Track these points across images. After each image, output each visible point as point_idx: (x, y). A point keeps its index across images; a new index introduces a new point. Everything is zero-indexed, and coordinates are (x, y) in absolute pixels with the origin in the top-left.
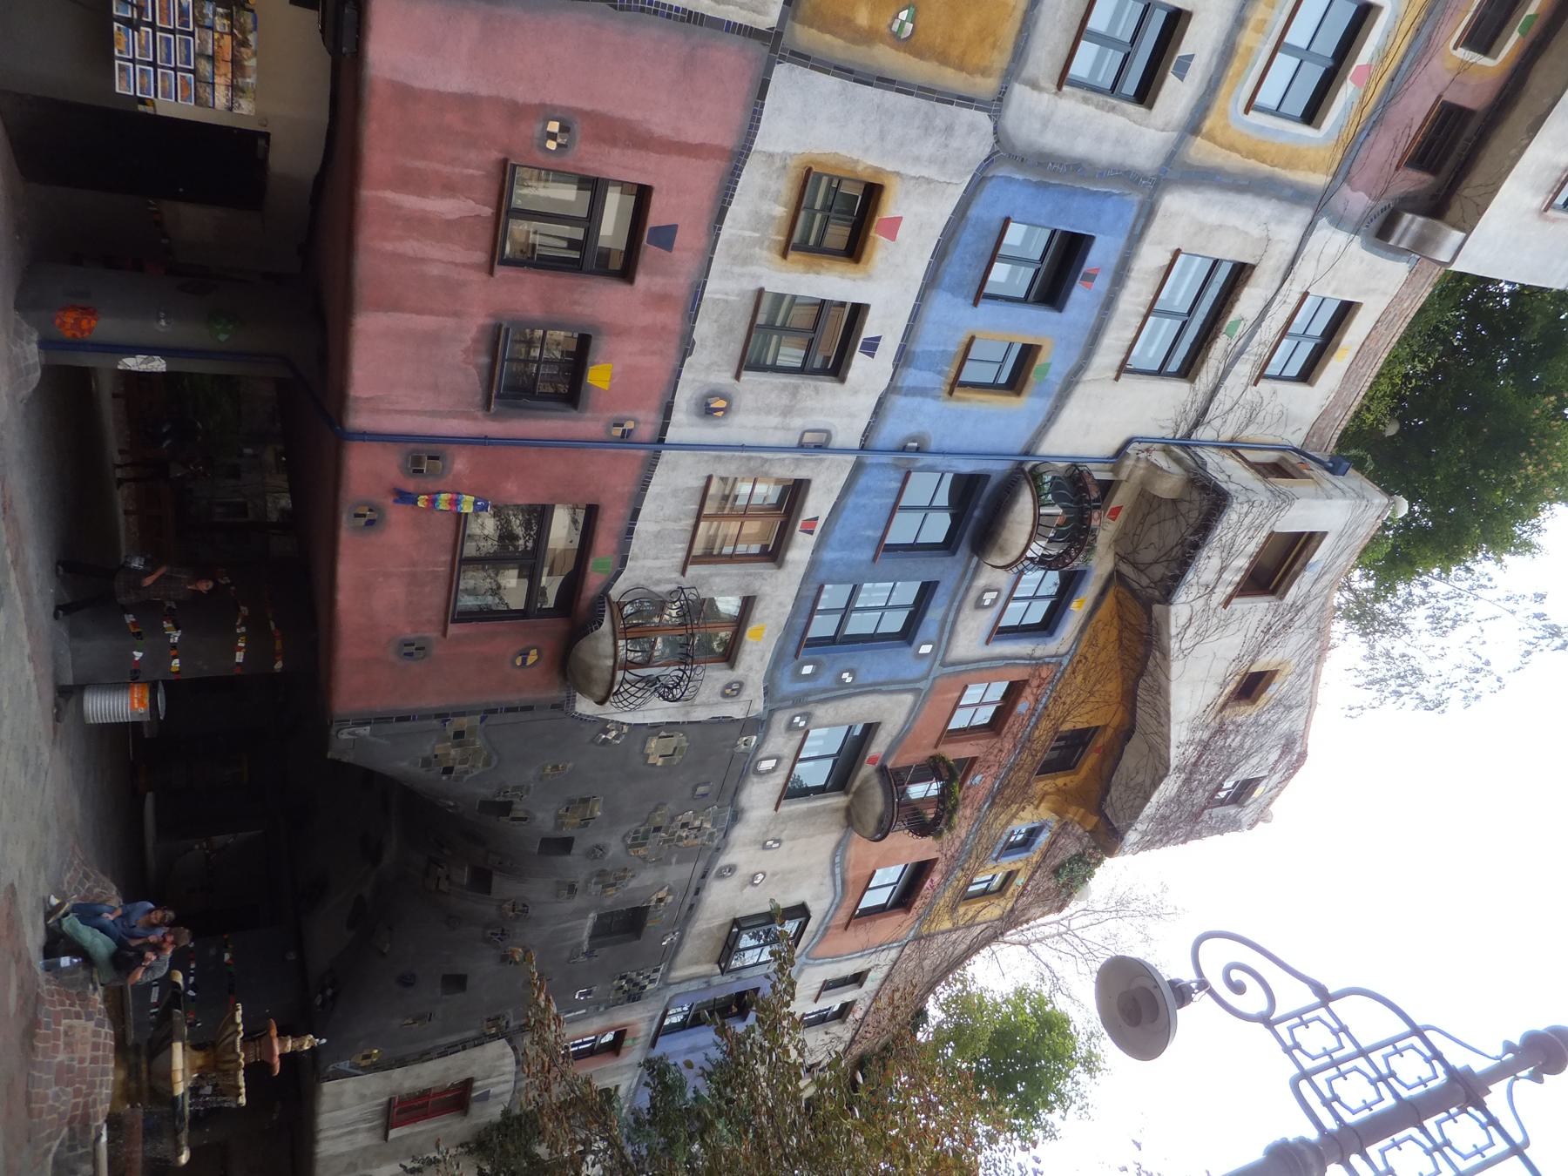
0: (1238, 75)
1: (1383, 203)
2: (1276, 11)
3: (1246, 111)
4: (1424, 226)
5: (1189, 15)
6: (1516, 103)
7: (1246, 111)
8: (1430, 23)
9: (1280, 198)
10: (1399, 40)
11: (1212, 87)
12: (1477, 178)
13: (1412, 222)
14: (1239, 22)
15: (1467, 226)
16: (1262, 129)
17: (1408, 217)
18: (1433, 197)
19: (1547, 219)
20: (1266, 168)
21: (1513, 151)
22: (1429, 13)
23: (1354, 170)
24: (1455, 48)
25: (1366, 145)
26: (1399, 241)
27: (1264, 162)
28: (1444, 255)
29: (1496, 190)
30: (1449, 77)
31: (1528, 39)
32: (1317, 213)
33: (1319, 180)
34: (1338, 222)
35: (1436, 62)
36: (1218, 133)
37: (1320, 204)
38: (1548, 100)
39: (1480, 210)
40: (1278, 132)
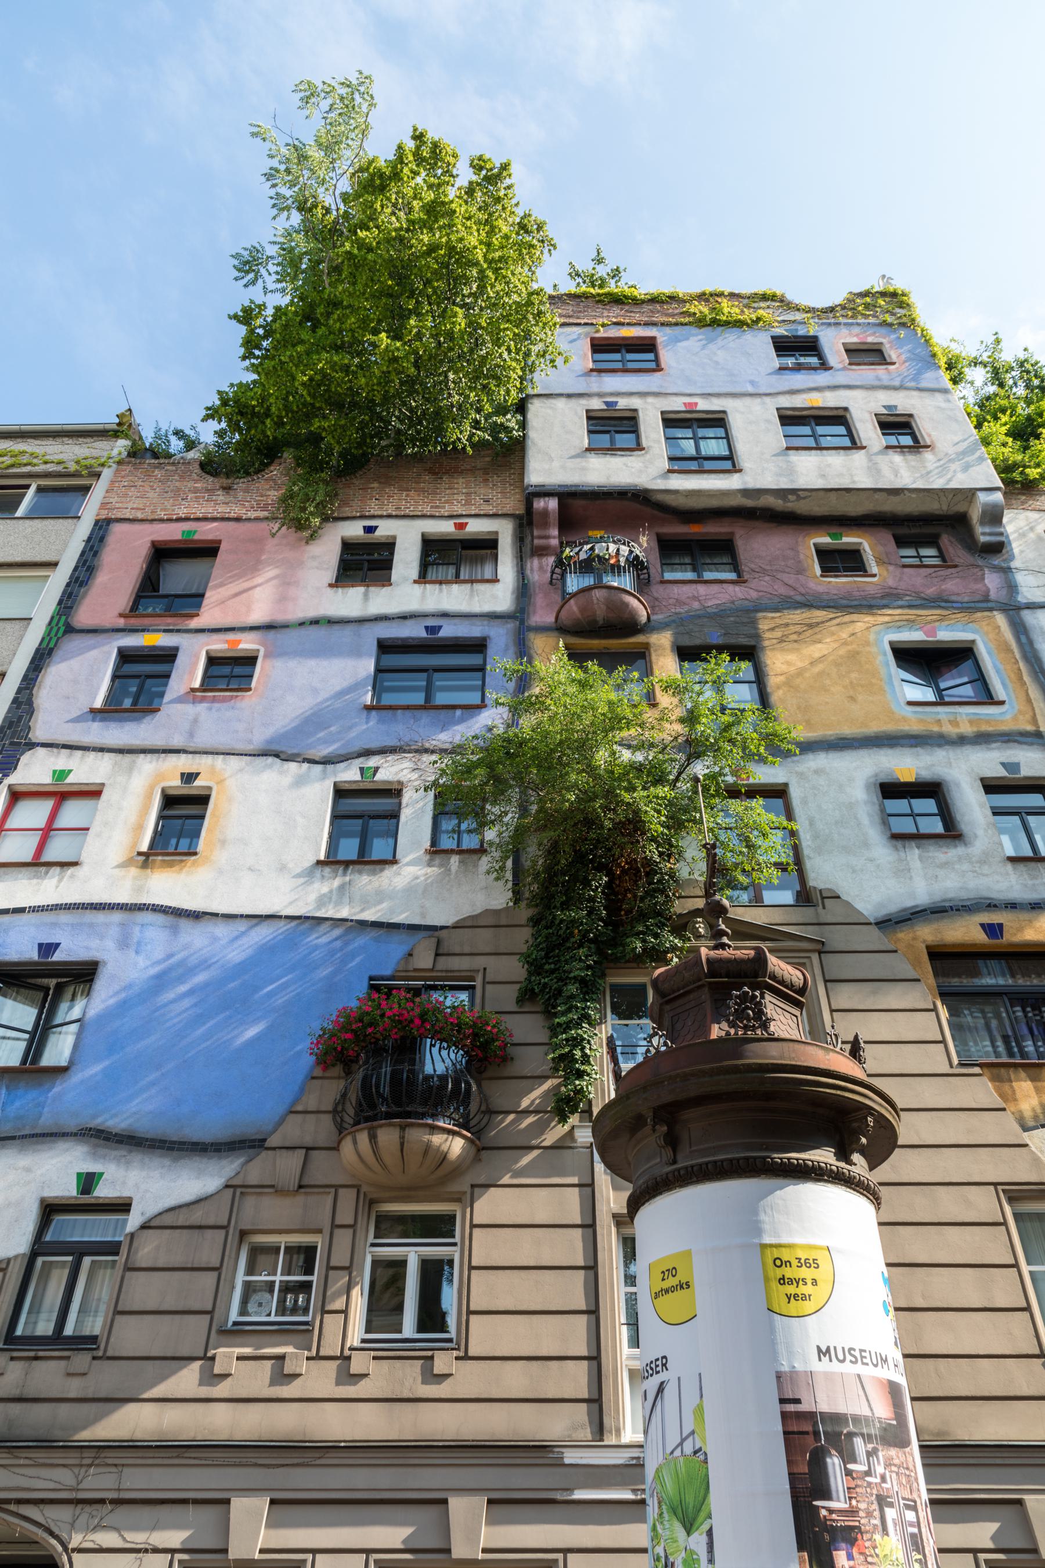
0: (988, 722)
1: (980, 562)
2: (939, 717)
3: (1002, 703)
4: (982, 523)
5: (982, 780)
7: (1002, 703)
8: (873, 602)
9: (1031, 642)
10: (897, 618)
11: (1009, 738)
12: (933, 507)
13: (983, 534)
14: (961, 741)
15: (970, 494)
16: (1004, 684)
17: (983, 539)
18: (953, 527)
19: (932, 442)
20: (1022, 665)
22: (871, 607)
23: (978, 598)
24: (874, 576)
25: (959, 599)
27: (1020, 670)
28: (998, 497)
29: (941, 490)
30: (891, 568)
31: (842, 530)
32: (1020, 608)
33: (1000, 619)
34: (1012, 588)
35: (891, 582)
36: (1028, 716)
37: (1014, 609)
38: (877, 496)
39: (956, 492)
40: (998, 671)
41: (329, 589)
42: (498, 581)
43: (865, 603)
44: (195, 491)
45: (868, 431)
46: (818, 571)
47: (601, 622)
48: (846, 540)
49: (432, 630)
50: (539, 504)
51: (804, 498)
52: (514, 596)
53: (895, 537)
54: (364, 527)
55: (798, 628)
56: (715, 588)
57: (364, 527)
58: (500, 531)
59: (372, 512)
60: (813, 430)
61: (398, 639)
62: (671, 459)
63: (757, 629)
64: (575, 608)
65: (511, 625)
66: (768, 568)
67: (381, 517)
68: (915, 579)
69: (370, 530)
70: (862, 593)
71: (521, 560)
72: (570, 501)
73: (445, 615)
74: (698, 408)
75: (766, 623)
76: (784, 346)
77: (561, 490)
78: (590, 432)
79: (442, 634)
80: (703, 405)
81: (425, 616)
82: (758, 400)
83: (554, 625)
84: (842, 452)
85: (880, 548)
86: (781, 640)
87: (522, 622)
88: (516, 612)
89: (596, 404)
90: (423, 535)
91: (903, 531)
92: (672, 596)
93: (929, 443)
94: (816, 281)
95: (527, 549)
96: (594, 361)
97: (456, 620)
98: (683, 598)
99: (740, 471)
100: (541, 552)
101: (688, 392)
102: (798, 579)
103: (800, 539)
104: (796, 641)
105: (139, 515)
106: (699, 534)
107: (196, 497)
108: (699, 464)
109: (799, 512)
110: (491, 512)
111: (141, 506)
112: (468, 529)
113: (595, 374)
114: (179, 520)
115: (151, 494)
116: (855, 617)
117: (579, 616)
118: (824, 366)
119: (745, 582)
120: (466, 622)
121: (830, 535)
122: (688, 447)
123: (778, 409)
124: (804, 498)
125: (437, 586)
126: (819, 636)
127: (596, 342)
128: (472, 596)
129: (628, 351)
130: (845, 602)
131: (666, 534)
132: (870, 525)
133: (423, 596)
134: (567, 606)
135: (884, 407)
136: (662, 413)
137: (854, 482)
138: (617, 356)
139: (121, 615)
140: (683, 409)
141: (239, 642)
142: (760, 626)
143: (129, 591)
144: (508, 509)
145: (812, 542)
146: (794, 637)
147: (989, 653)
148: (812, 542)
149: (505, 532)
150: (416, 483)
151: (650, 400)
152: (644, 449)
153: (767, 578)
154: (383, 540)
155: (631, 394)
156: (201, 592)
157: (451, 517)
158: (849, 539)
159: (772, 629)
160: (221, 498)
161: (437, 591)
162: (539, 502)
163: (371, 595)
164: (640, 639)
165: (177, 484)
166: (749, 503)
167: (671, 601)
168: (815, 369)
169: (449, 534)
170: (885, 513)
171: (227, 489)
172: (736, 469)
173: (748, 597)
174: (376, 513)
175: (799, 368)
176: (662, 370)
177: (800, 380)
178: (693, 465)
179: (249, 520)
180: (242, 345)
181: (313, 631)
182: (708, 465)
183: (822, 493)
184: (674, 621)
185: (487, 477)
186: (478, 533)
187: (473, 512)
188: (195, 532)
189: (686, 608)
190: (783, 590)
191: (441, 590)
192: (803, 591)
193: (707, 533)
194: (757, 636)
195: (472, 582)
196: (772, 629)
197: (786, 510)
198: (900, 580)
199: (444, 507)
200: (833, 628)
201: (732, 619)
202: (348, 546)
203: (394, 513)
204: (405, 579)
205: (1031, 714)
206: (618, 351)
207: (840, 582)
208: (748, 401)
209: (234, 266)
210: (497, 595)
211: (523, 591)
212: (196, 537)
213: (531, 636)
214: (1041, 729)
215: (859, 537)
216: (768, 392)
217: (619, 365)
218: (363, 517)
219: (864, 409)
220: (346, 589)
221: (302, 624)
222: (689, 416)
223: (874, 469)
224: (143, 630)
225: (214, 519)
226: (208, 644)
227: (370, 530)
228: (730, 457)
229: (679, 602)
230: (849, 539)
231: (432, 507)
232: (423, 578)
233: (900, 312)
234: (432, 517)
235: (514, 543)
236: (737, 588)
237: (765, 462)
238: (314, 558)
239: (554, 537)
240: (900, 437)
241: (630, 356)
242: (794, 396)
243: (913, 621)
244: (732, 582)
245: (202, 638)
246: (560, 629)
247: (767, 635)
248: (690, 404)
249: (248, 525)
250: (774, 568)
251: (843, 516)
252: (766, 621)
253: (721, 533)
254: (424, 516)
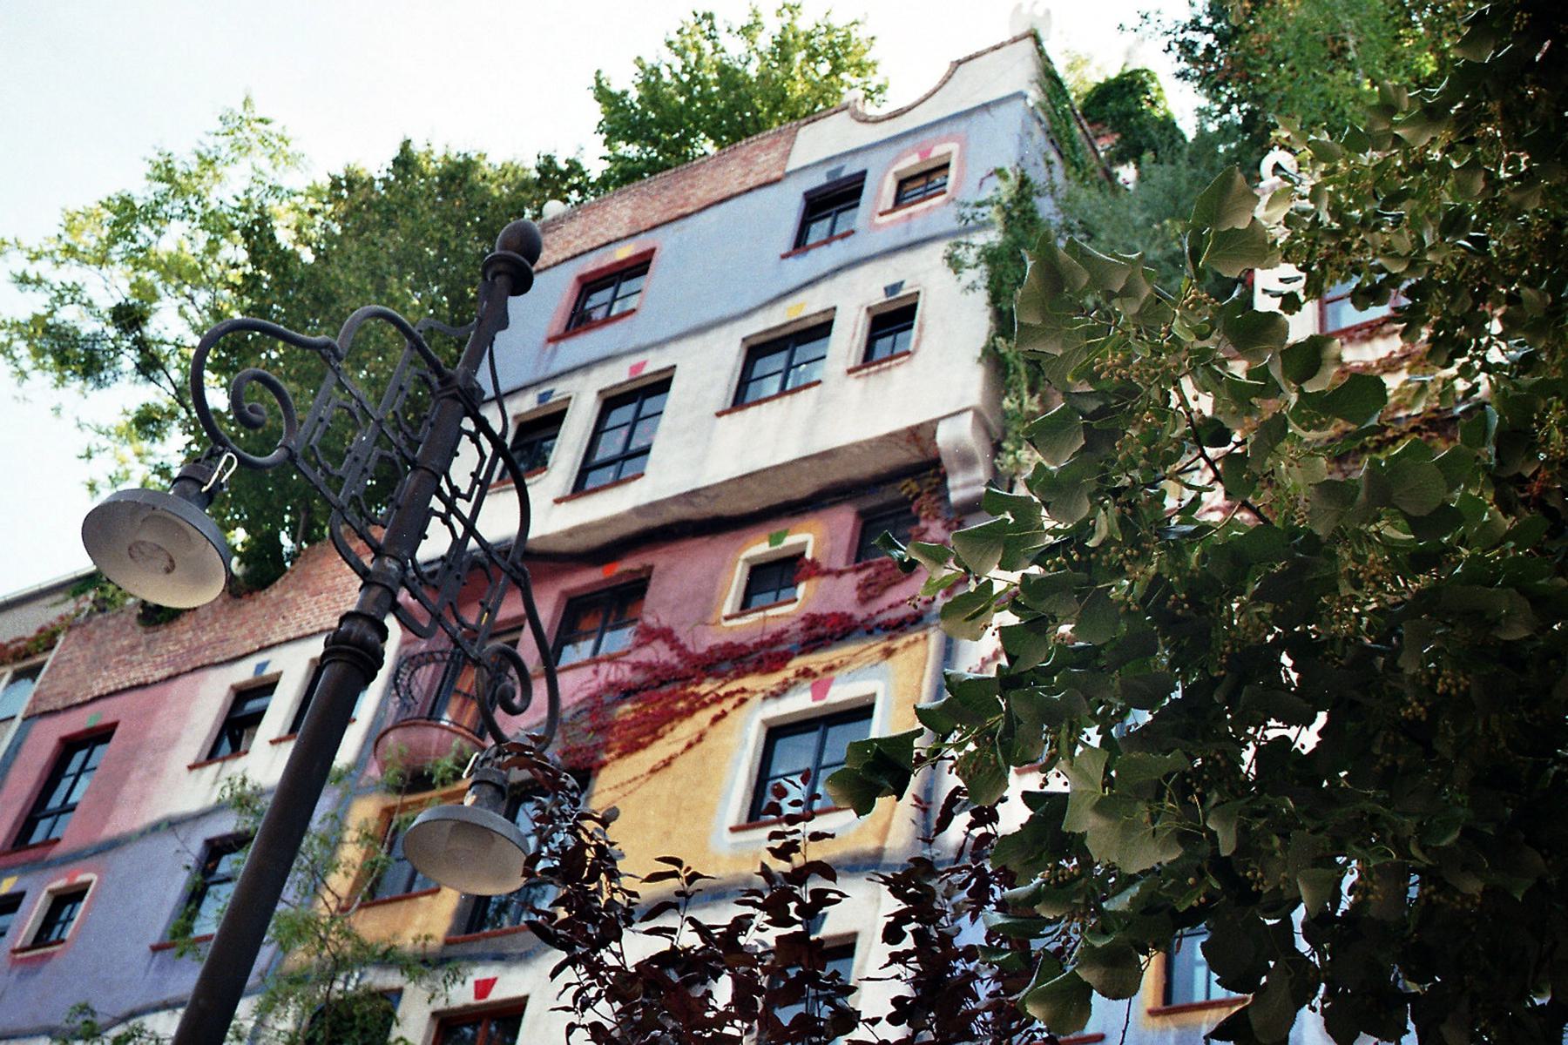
4: (954, 473)
13: (955, 488)
19: (918, 343)
21: (856, 450)
26: (979, 482)
38: (806, 465)
48: (791, 540)
51: (717, 496)
53: (861, 514)
59: (274, 640)
67: (280, 644)
80: (654, 362)
82: (725, 331)
109: (727, 513)
124: (717, 496)
132: (833, 504)
147: (883, 715)
166: (653, 521)
179: (155, 683)
183: (733, 487)
205: (886, 819)
214: (887, 845)
225: (125, 690)
245: (51, 873)
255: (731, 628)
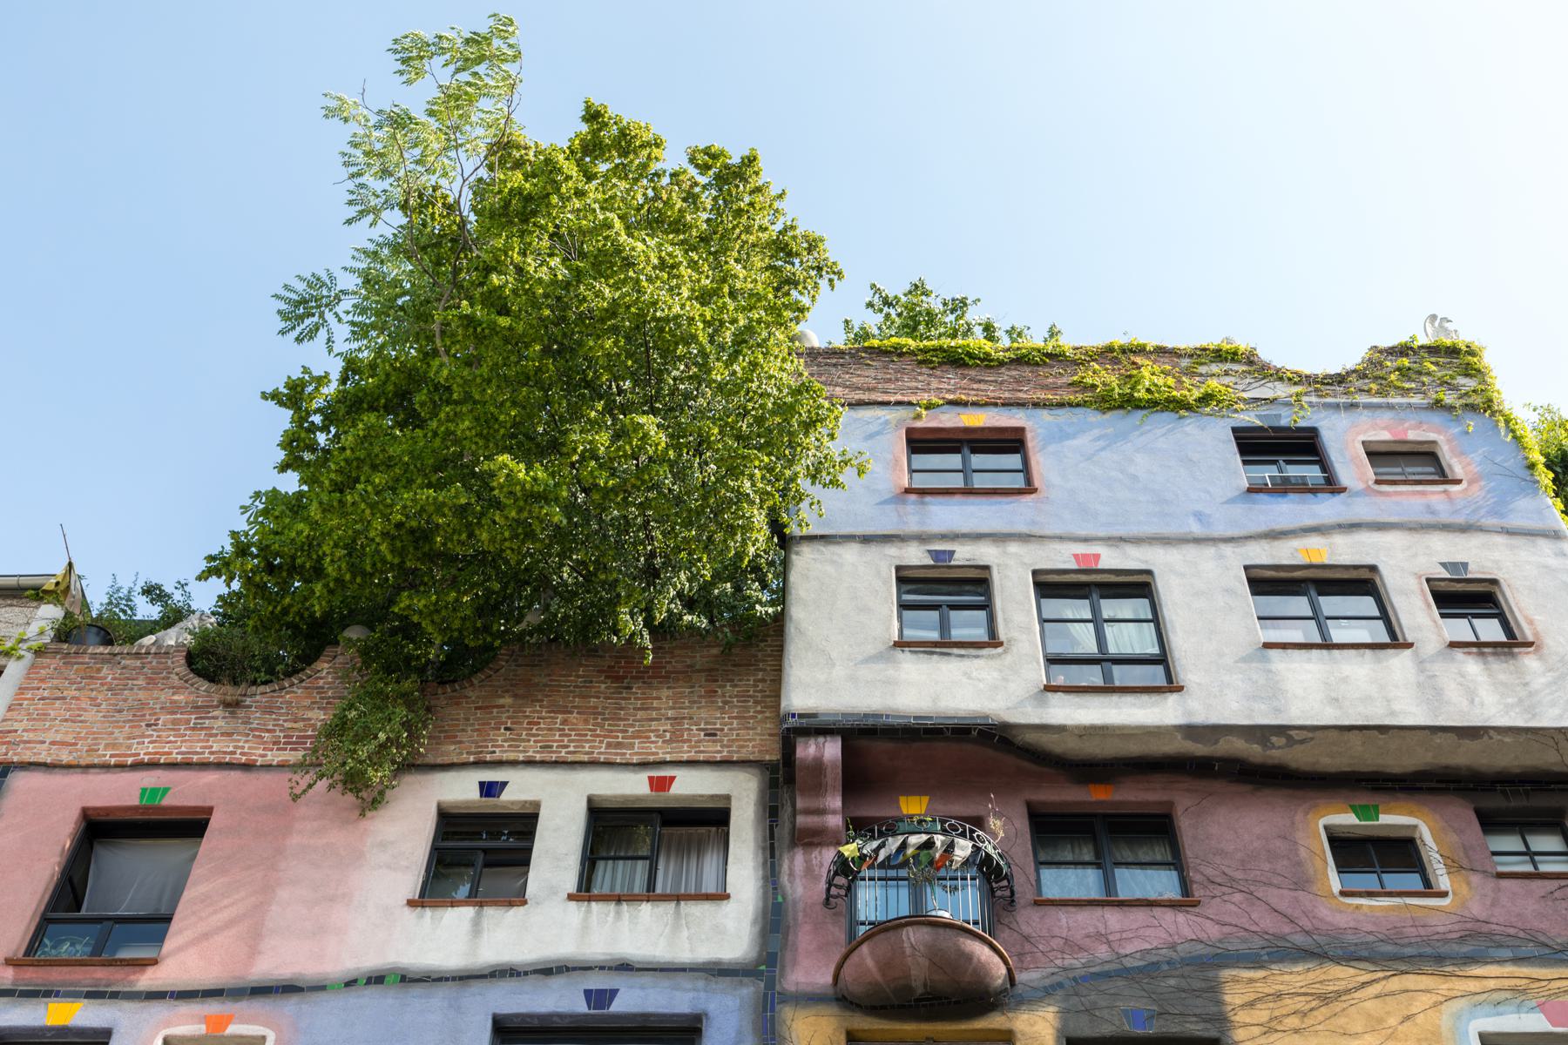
6: (1447, 767)
8: (1444, 949)
10: (1492, 984)
19: (1536, 634)
22: (1440, 959)
24: (1444, 894)
30: (1475, 879)
35: (1476, 910)
38: (1438, 739)
41: (407, 910)
42: (727, 897)
43: (1429, 950)
44: (174, 708)
45: (1416, 612)
46: (1335, 882)
47: (920, 991)
48: (1386, 819)
49: (599, 998)
50: (807, 750)
51: (1302, 742)
52: (757, 928)
54: (482, 784)
55: (1300, 1003)
56: (1139, 916)
57: (482, 784)
58: (734, 794)
59: (498, 755)
60: (1314, 607)
61: (531, 1016)
62: (1053, 661)
63: (1220, 1003)
64: (870, 963)
65: (748, 991)
66: (1238, 875)
67: (513, 763)
68: (1523, 906)
69: (489, 789)
70: (1422, 931)
71: (773, 856)
72: (864, 743)
73: (624, 967)
74: (1100, 567)
75: (1240, 990)
76: (1256, 445)
77: (848, 724)
78: (903, 606)
79: (617, 1006)
80: (1111, 559)
81: (585, 968)
82: (1209, 551)
83: (830, 991)
84: (1368, 652)
85: (1453, 838)
86: (1268, 1029)
87: (770, 984)
88: (758, 962)
89: (915, 556)
90: (590, 800)
91: (1494, 802)
92: (1056, 931)
93: (1531, 639)
94: (1314, 332)
95: (784, 831)
96: (912, 471)
97: (646, 979)
98: (1078, 936)
99: (1180, 689)
100: (810, 839)
101: (1083, 533)
102: (1296, 899)
103: (1299, 817)
104: (1296, 1031)
105: (65, 757)
106: (1109, 803)
107: (174, 722)
108: (1106, 670)
109: (1293, 765)
110: (718, 757)
111: (70, 739)
112: (677, 789)
113: (913, 497)
114: (138, 766)
115: (91, 715)
116: (1410, 981)
117: (878, 977)
118: (1331, 485)
119: (1195, 904)
120: (665, 982)
121: (1355, 810)
122: (1084, 640)
123: (1246, 568)
124: (1302, 742)
125: (612, 906)
126: (1342, 1021)
127: (916, 436)
128: (676, 927)
129: (974, 451)
130: (1389, 948)
131: (1044, 803)
132: (1431, 791)
133: (585, 928)
134: (854, 957)
135: (1444, 565)
136: (1035, 573)
137: (1393, 713)
138: (954, 460)
139: (9, 962)
140: (1074, 566)
141: (229, 1020)
142: (1227, 998)
143: (29, 913)
144: (750, 751)
145: (1322, 822)
146: (1293, 1022)
148: (1322, 822)
149: (743, 795)
150: (584, 697)
151: (1013, 548)
152: (1001, 644)
153: (1238, 897)
154: (516, 809)
155: (978, 537)
156: (163, 911)
157: (644, 765)
158: (1393, 819)
159: (1251, 1005)
160: (220, 723)
161: (612, 914)
162: (806, 746)
163: (485, 923)
164: (995, 1021)
165: (142, 695)
166: (1199, 749)
167: (1056, 943)
168: (1314, 491)
169: (638, 798)
170: (1458, 768)
171: (232, 706)
172: (1172, 686)
173: (1203, 936)
174: (505, 757)
175: (1284, 488)
176: (1034, 491)
177: (1287, 511)
178: (1093, 675)
179: (268, 767)
180: (282, 445)
181: (370, 998)
182: (1121, 675)
183: (1335, 733)
184: (1060, 985)
185: (714, 686)
186: (694, 797)
187: (685, 757)
188: (166, 790)
189: (1084, 958)
190: (1268, 923)
191: (618, 913)
192: (1308, 925)
193: (1121, 803)
194: (1221, 1020)
195: (678, 898)
196: (1251, 1005)
197: (1270, 762)
198: (1493, 905)
199: (632, 746)
200: (1368, 1004)
201: (1172, 982)
202: (451, 823)
203: (538, 757)
204: (553, 891)
206: (955, 450)
207: (1376, 907)
208: (1191, 551)
209: (279, 312)
210: (725, 929)
211: (774, 919)
212: (168, 801)
213: (787, 1012)
215: (1411, 814)
216: (1229, 533)
217: (957, 481)
218: (480, 764)
219: (1406, 566)
220: (440, 912)
221: (351, 983)
222: (1084, 578)
223: (1430, 689)
224: (48, 994)
225: (204, 766)
226: (168, 1024)
227: (489, 789)
228: (1162, 659)
229: (1070, 945)
230: (1393, 819)
231: (609, 745)
232: (585, 891)
233: (1469, 384)
234: (609, 764)
235: (759, 820)
236: (1181, 917)
237: (1231, 671)
238: (383, 845)
239: (834, 812)
240: (1476, 622)
241: (978, 460)
242: (1276, 543)
243: (1524, 991)
244: (1172, 905)
245: (159, 1010)
246: (843, 999)
247: (1241, 1017)
248: (1085, 556)
249: (266, 778)
250: (1252, 875)
251: (1376, 773)
252: (1239, 988)
253: (1147, 804)
254: (594, 764)
255: (1358, 907)
